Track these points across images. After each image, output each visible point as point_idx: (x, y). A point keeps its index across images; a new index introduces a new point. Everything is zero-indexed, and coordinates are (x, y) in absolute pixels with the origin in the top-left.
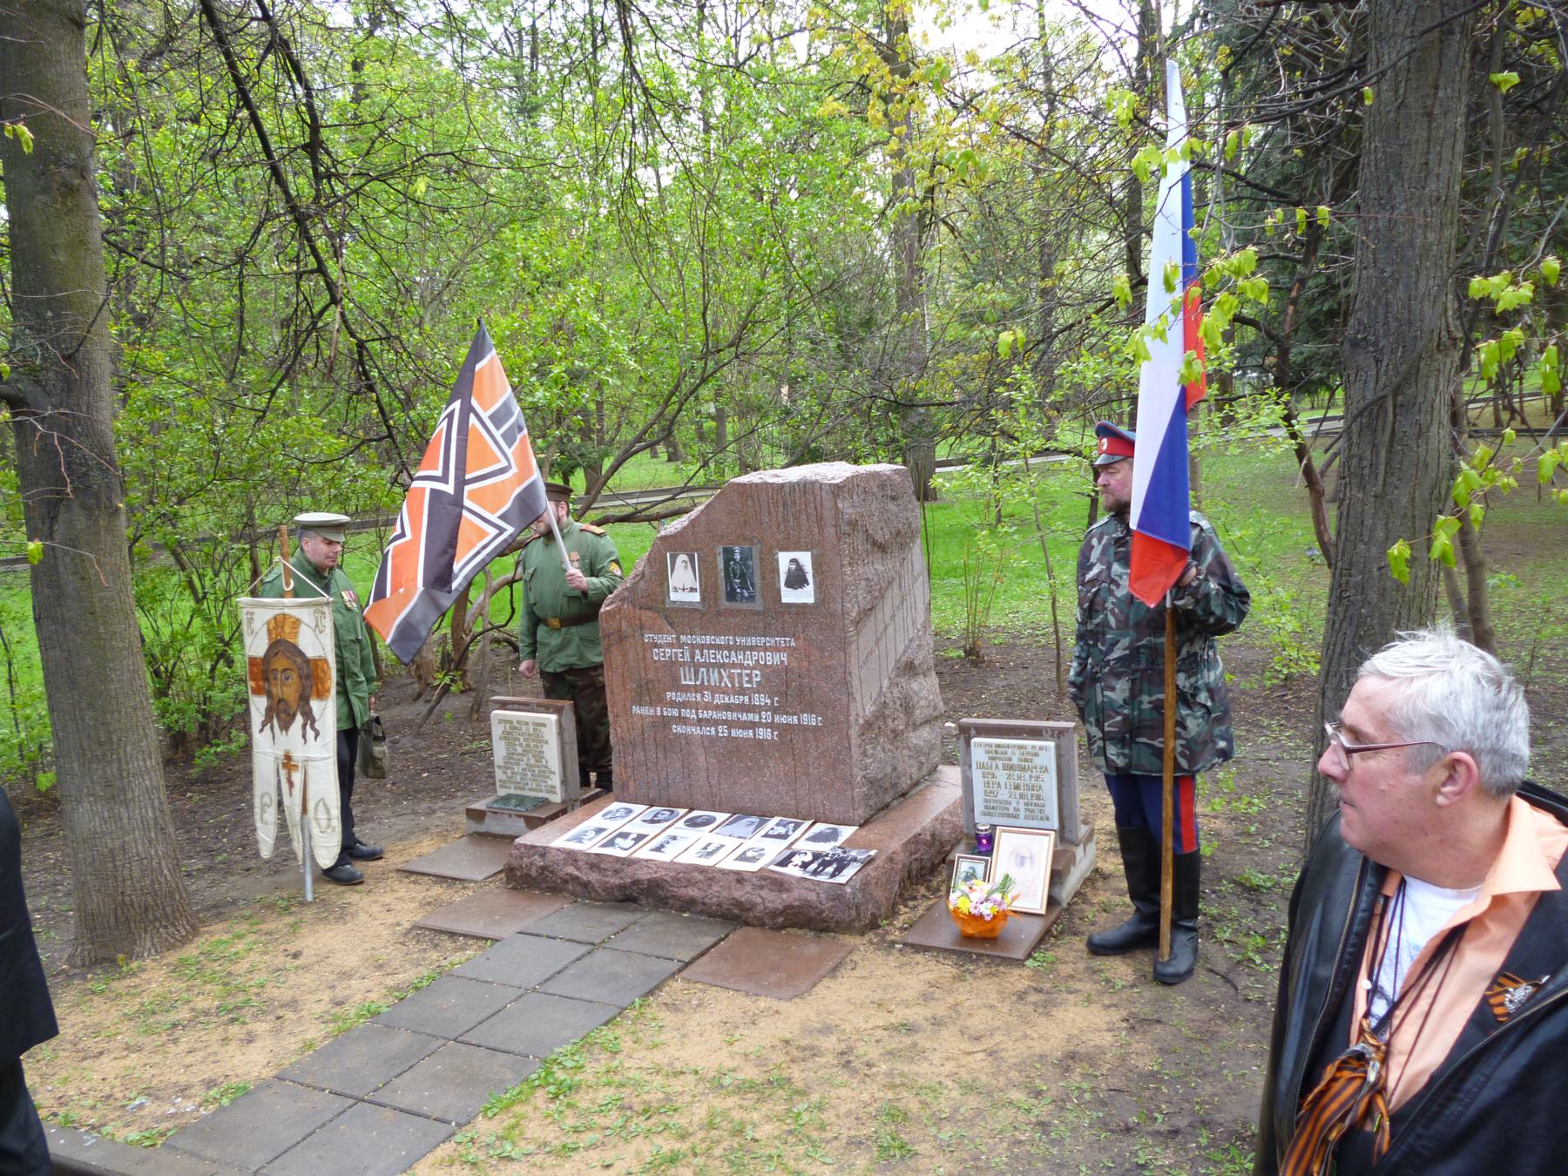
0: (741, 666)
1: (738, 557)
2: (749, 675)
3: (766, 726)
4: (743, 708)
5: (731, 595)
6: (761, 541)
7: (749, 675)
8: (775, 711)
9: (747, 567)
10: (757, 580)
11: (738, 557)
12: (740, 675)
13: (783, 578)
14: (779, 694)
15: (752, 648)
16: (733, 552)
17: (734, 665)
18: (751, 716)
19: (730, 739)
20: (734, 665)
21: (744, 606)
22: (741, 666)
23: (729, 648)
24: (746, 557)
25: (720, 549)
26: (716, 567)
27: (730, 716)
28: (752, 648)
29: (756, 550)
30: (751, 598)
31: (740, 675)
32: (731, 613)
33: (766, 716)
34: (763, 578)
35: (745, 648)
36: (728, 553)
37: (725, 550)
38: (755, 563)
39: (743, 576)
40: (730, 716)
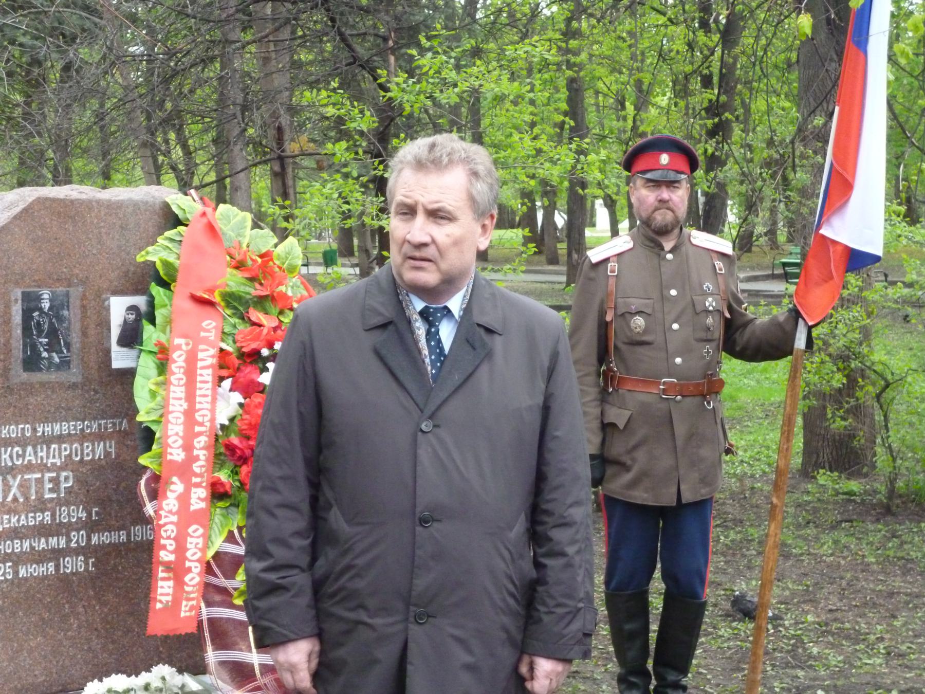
0: (43, 468)
1: (46, 305)
2: (55, 481)
3: (77, 552)
4: (43, 531)
5: (32, 362)
6: (84, 282)
7: (55, 481)
8: (91, 527)
9: (60, 319)
10: (75, 339)
11: (46, 305)
12: (40, 481)
13: (115, 332)
14: (102, 503)
15: (60, 439)
16: (39, 298)
17: (29, 468)
18: (53, 541)
19: (17, 582)
20: (29, 468)
21: (53, 377)
22: (43, 468)
23: (22, 442)
24: (58, 306)
25: (18, 293)
26: (8, 322)
27: (19, 546)
28: (60, 439)
29: (76, 293)
30: (65, 364)
31: (40, 481)
32: (29, 388)
33: (78, 538)
34: (84, 334)
35: (48, 441)
36: (31, 302)
37: (26, 297)
38: (72, 315)
39: (53, 333)
40: (19, 546)
